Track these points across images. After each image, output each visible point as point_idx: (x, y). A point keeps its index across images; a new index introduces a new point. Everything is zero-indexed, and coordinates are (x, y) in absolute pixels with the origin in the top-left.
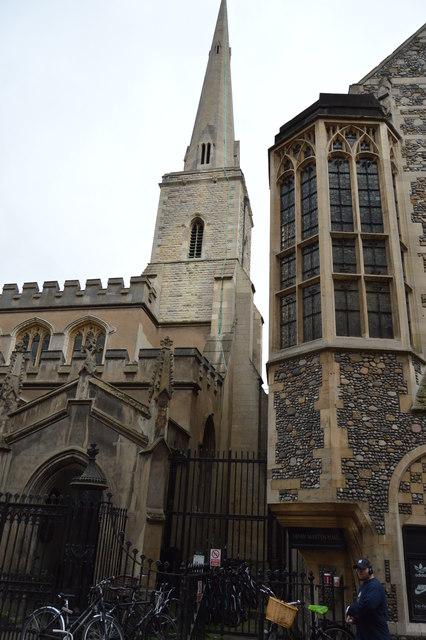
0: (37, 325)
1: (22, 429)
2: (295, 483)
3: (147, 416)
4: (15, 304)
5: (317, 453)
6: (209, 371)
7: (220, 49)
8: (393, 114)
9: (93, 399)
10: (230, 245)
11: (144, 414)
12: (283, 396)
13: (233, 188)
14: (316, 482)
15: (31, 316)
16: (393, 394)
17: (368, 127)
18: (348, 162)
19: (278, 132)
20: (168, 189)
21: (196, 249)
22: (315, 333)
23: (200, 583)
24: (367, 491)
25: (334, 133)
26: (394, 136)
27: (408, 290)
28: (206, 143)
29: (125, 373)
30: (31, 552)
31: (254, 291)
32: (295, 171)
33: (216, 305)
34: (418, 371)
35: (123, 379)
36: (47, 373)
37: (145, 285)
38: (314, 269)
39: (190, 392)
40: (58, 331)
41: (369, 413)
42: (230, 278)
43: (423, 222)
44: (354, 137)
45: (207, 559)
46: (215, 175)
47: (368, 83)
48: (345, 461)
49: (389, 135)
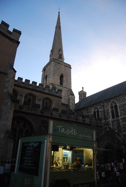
7: (58, 28)
15: (30, 91)
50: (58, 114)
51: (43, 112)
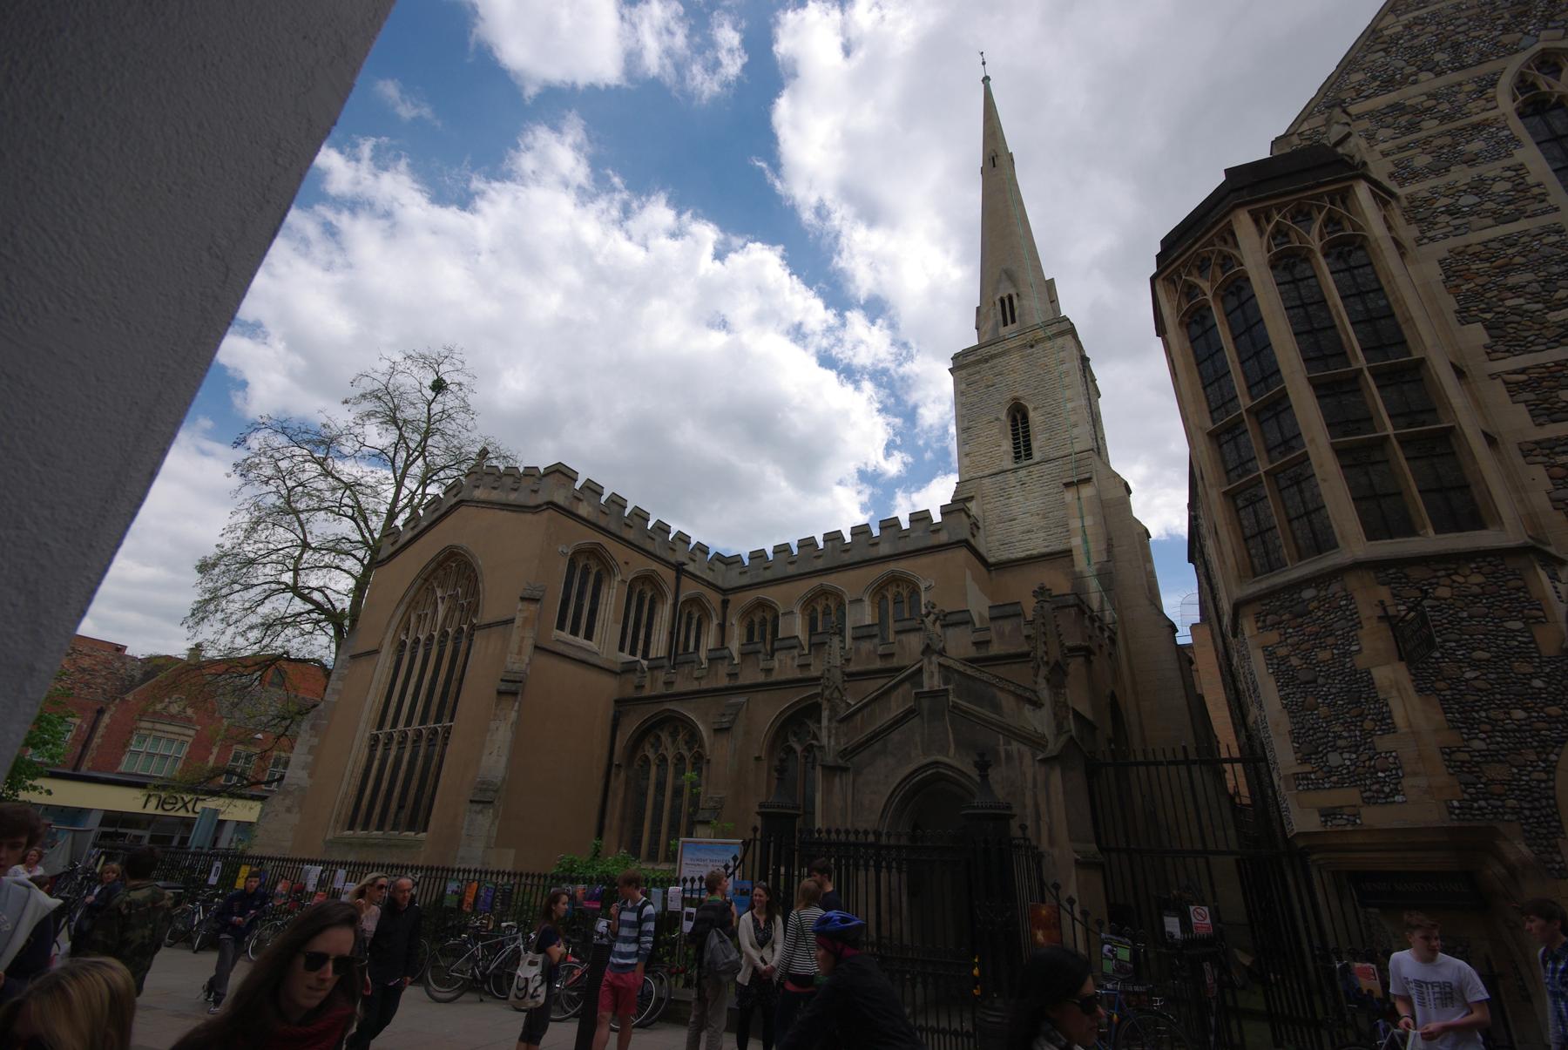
0: (823, 593)
1: (861, 737)
2: (1348, 796)
3: (1037, 704)
4: (792, 570)
5: (1383, 743)
6: (1097, 624)
8: (1368, 159)
9: (950, 687)
10: (1076, 431)
11: (1030, 701)
12: (1282, 651)
13: (1063, 348)
14: (1395, 791)
15: (815, 582)
16: (1518, 625)
17: (1332, 196)
18: (1307, 260)
19: (1158, 250)
20: (964, 373)
21: (1022, 447)
22: (1322, 541)
23: (1207, 966)
24: (1511, 803)
25: (1268, 222)
26: (1383, 196)
27: (1491, 440)
28: (1005, 295)
29: (975, 644)
30: (905, 912)
31: (1129, 491)
32: (1209, 296)
33: (1075, 524)
34: (1554, 578)
35: (972, 652)
36: (867, 655)
37: (963, 515)
38: (1291, 441)
39: (1081, 660)
40: (855, 597)
41: (1475, 665)
42: (1088, 480)
43: (1483, 321)
44: (1308, 217)
45: (1186, 924)
46: (1030, 336)
47: (1305, 127)
48: (1448, 752)
49: (1375, 195)
50: (793, 658)
51: (736, 674)
